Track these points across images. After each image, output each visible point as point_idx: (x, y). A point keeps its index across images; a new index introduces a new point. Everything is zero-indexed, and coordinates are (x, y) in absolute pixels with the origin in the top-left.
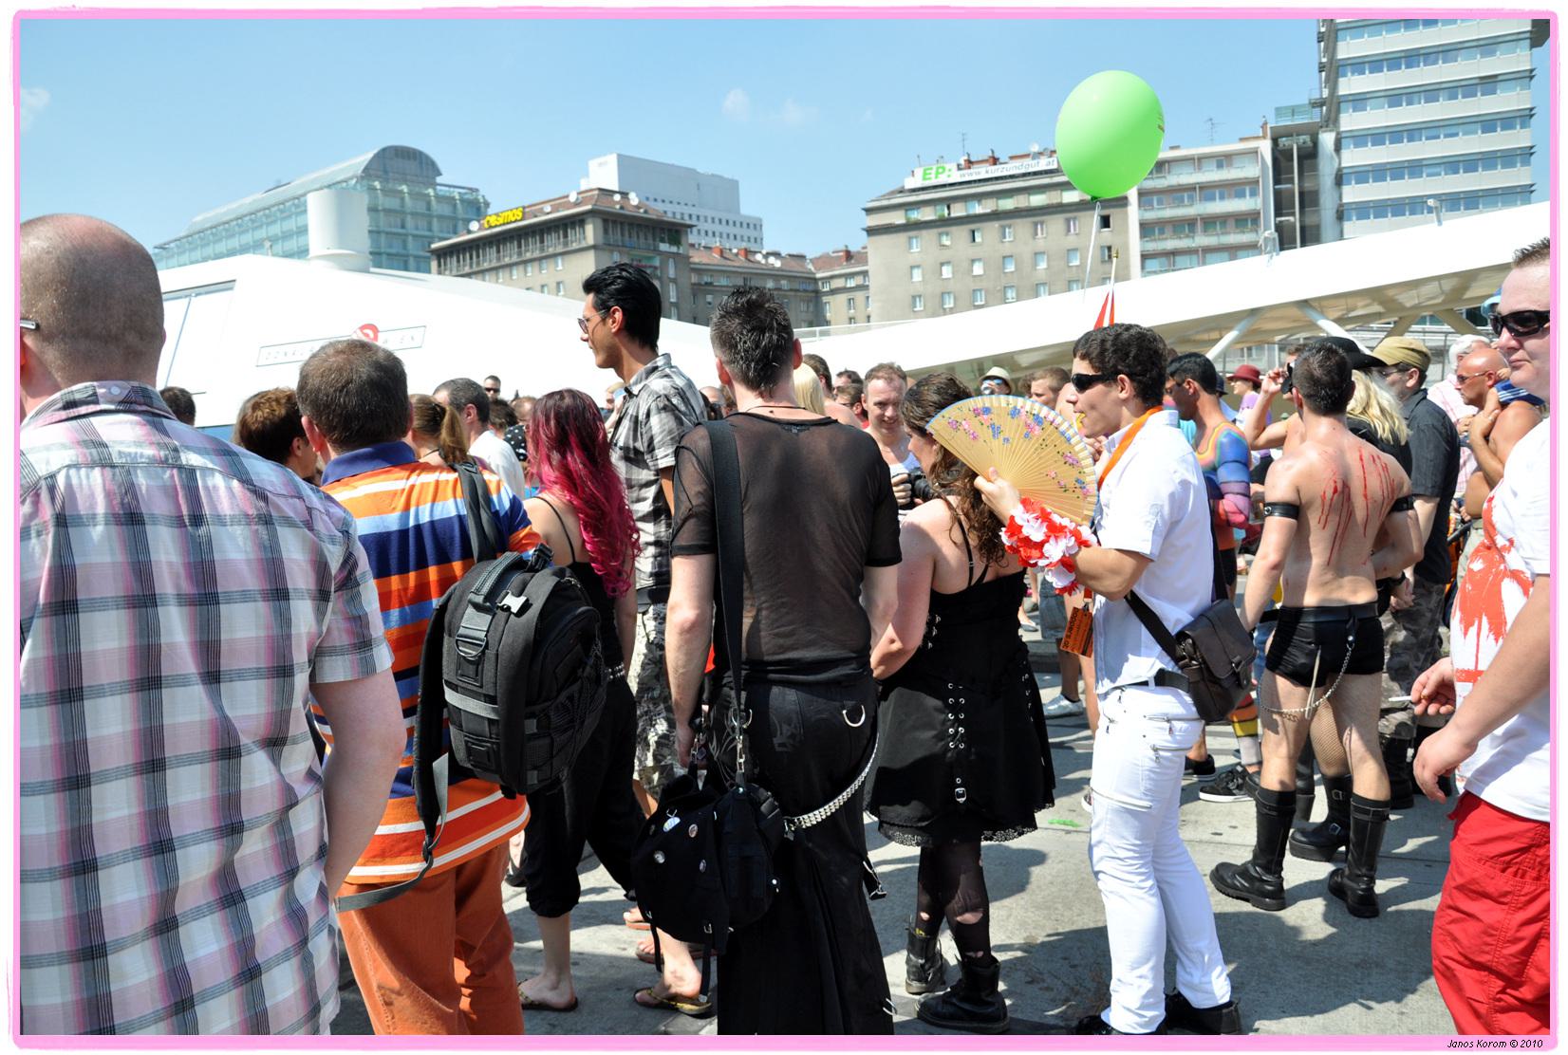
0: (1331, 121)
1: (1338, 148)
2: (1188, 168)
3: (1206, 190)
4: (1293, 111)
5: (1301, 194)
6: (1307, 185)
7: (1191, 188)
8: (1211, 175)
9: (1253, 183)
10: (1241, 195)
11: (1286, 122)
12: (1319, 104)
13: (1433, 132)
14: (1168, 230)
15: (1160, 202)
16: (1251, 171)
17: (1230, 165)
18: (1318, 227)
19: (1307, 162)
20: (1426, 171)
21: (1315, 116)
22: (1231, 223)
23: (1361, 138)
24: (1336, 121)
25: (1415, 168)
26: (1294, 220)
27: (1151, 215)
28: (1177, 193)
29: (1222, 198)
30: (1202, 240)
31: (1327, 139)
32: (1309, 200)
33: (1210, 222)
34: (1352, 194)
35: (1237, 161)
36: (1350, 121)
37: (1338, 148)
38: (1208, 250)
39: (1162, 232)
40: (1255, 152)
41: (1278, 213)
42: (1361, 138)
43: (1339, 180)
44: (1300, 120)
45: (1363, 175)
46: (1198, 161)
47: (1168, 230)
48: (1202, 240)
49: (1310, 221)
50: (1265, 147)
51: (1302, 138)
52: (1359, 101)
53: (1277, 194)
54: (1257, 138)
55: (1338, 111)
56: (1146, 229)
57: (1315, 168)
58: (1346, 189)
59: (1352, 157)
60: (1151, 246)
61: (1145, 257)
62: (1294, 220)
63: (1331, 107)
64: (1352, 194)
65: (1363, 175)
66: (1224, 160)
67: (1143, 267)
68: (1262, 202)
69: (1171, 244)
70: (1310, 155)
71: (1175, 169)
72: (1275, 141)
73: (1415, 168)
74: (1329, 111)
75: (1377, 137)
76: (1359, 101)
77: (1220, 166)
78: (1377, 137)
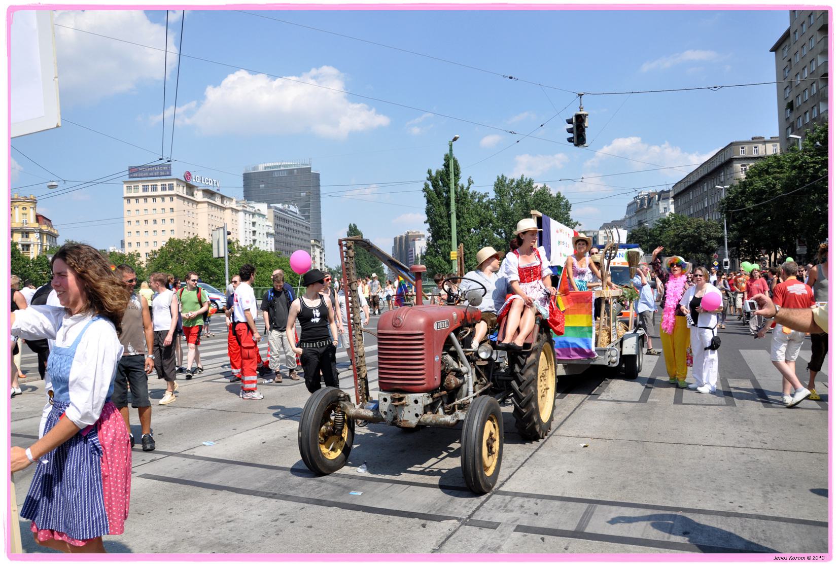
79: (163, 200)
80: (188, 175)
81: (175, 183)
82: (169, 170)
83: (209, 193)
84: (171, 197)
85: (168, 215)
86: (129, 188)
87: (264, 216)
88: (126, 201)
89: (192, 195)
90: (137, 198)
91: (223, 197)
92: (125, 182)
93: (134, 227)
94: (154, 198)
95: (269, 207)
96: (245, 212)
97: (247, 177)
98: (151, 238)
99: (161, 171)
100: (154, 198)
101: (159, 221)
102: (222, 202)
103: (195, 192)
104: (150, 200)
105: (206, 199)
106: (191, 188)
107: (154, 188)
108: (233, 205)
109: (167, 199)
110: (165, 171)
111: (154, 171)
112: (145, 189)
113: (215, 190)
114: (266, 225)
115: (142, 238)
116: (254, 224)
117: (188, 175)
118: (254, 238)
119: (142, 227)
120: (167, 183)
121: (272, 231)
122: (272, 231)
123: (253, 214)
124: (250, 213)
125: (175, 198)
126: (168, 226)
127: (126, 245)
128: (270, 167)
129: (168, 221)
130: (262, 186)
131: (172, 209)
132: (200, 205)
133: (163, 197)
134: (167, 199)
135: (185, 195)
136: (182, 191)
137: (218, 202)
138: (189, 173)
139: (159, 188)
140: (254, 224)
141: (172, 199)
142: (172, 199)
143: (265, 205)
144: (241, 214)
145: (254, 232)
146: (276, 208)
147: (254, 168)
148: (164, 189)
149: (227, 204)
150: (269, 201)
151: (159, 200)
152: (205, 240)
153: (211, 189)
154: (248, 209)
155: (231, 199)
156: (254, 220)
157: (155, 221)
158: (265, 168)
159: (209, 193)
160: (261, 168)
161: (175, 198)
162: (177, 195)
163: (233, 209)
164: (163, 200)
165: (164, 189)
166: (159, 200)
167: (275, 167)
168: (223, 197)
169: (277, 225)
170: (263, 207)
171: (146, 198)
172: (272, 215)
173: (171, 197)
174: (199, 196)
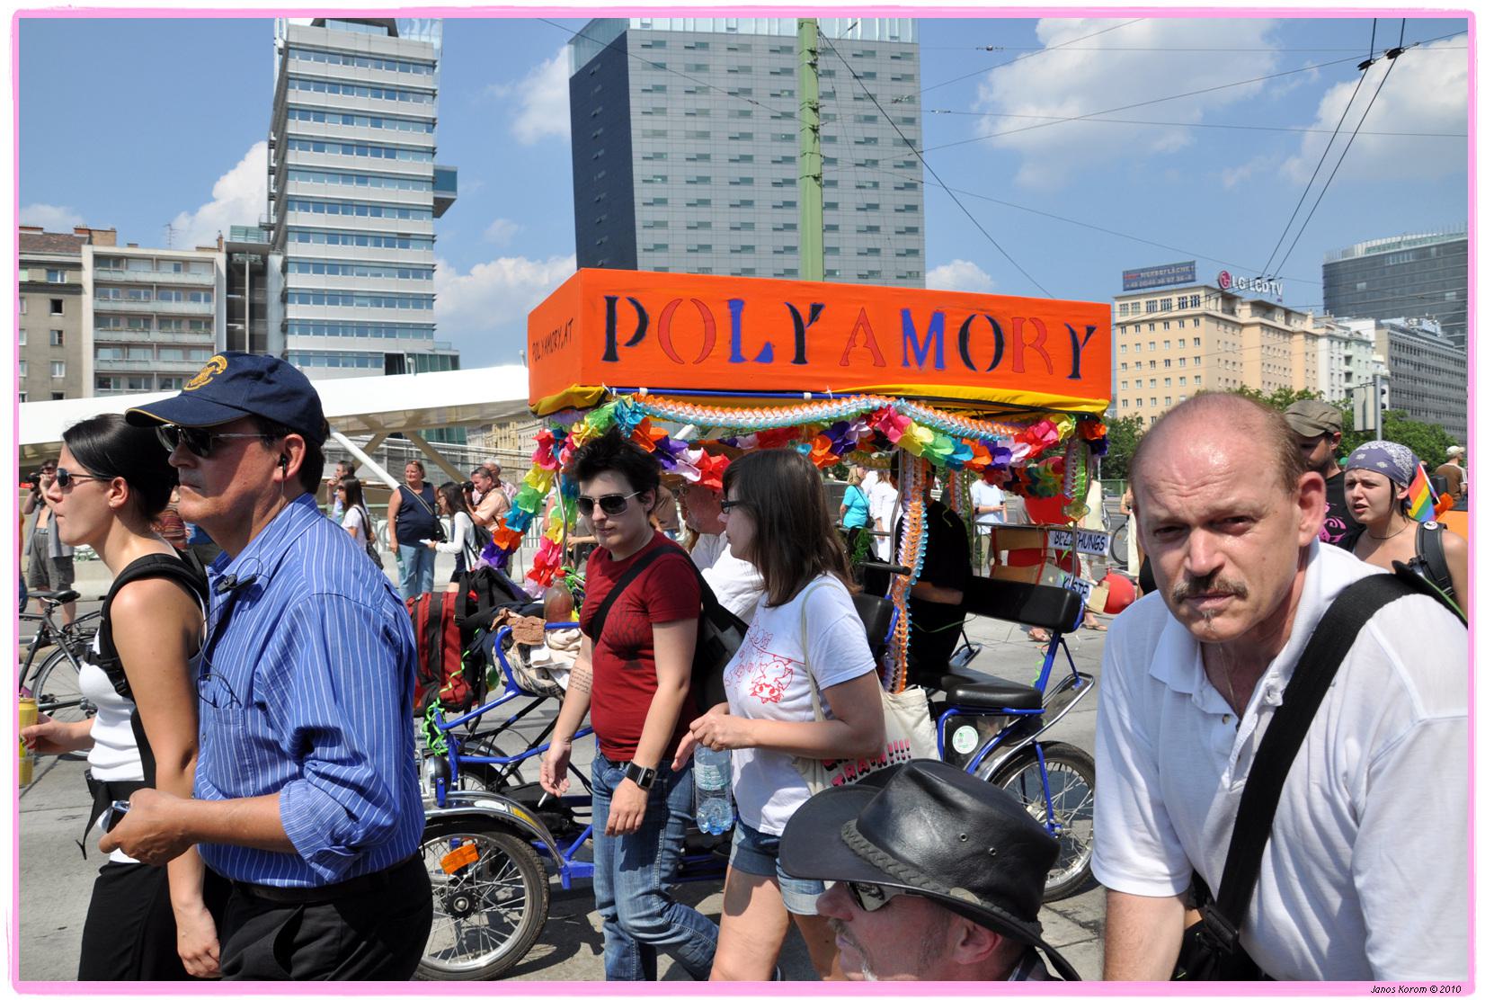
0: (280, 244)
1: (284, 270)
2: (146, 266)
3: (163, 290)
4: (247, 231)
5: (252, 306)
6: (257, 298)
7: (148, 286)
8: (167, 276)
9: (211, 289)
10: (196, 299)
11: (239, 240)
12: (269, 227)
13: (363, 270)
14: (123, 324)
15: (116, 295)
16: (207, 279)
17: (187, 270)
18: (265, 337)
19: (257, 279)
20: (356, 301)
21: (265, 239)
22: (186, 324)
23: (305, 265)
24: (283, 246)
25: (346, 297)
26: (244, 327)
27: (107, 306)
28: (134, 288)
29: (178, 299)
30: (156, 336)
31: (275, 261)
32: (258, 311)
33: (165, 320)
34: (295, 311)
35: (193, 267)
36: (295, 249)
37: (284, 270)
38: (162, 346)
39: (117, 323)
40: (211, 262)
41: (230, 318)
42: (305, 265)
43: (285, 298)
44: (252, 241)
45: (306, 296)
46: (157, 262)
47: (123, 324)
48: (156, 336)
49: (259, 329)
50: (221, 259)
51: (253, 257)
52: (305, 234)
53: (229, 301)
54: (212, 249)
55: (286, 239)
56: (100, 319)
57: (264, 284)
58: (290, 306)
59: (296, 281)
60: (106, 336)
61: (98, 346)
62: (244, 327)
63: (279, 233)
64: (295, 311)
65: (306, 296)
66: (181, 264)
67: (96, 356)
68: (215, 308)
69: (125, 336)
70: (260, 272)
71: (133, 265)
72: (229, 255)
73: (346, 297)
74: (276, 236)
75: (318, 266)
76: (305, 234)
77: (177, 269)
78: (318, 266)
79: (1182, 324)
80: (1225, 277)
81: (1202, 293)
82: (1192, 272)
83: (1263, 307)
84: (1196, 318)
85: (1191, 350)
86: (1124, 308)
87: (1367, 343)
88: (1118, 330)
89: (1233, 312)
90: (1137, 324)
91: (1288, 313)
92: (1117, 298)
93: (1133, 372)
94: (1166, 322)
95: (1379, 326)
96: (1332, 338)
97: (1332, 275)
98: (1161, 390)
99: (1182, 274)
100: (1166, 322)
101: (1175, 364)
102: (1287, 323)
103: (1238, 307)
104: (1159, 326)
105: (1258, 319)
106: (1229, 300)
107: (1167, 306)
108: (1308, 326)
109: (1189, 323)
110: (1184, 274)
111: (1167, 275)
112: (1151, 308)
113: (1273, 301)
114: (1374, 362)
115: (1146, 392)
116: (1348, 359)
117: (1225, 277)
118: (1348, 385)
119: (1147, 371)
120: (1188, 295)
121: (1384, 370)
122: (1384, 370)
123: (1347, 342)
124: (1340, 339)
125: (1202, 320)
126: (1191, 369)
127: (1120, 403)
128: (1379, 248)
129: (1190, 362)
130: (1362, 286)
131: (1197, 340)
132: (1246, 330)
133: (1181, 319)
134: (1189, 323)
135: (1220, 314)
136: (1214, 306)
137: (1279, 321)
138: (1226, 274)
139: (1175, 302)
140: (1348, 359)
141: (1197, 322)
142: (1197, 322)
143: (1371, 323)
144: (1323, 343)
145: (1348, 375)
146: (1393, 327)
147: (1344, 253)
148: (1182, 305)
149: (1296, 325)
150: (1378, 317)
151: (1174, 324)
152: (1259, 392)
153: (1266, 299)
154: (1338, 332)
155: (1303, 316)
156: (1349, 352)
157: (1168, 362)
158: (1368, 250)
159: (1263, 307)
160: (1360, 251)
161: (1202, 320)
162: (1207, 315)
163: (1307, 334)
164: (1182, 324)
165: (1182, 305)
166: (1174, 324)
167: (1389, 246)
168: (1288, 313)
169: (1394, 360)
170: (1366, 327)
171: (1151, 322)
172: (1386, 344)
173: (1196, 318)
174: (1244, 314)
